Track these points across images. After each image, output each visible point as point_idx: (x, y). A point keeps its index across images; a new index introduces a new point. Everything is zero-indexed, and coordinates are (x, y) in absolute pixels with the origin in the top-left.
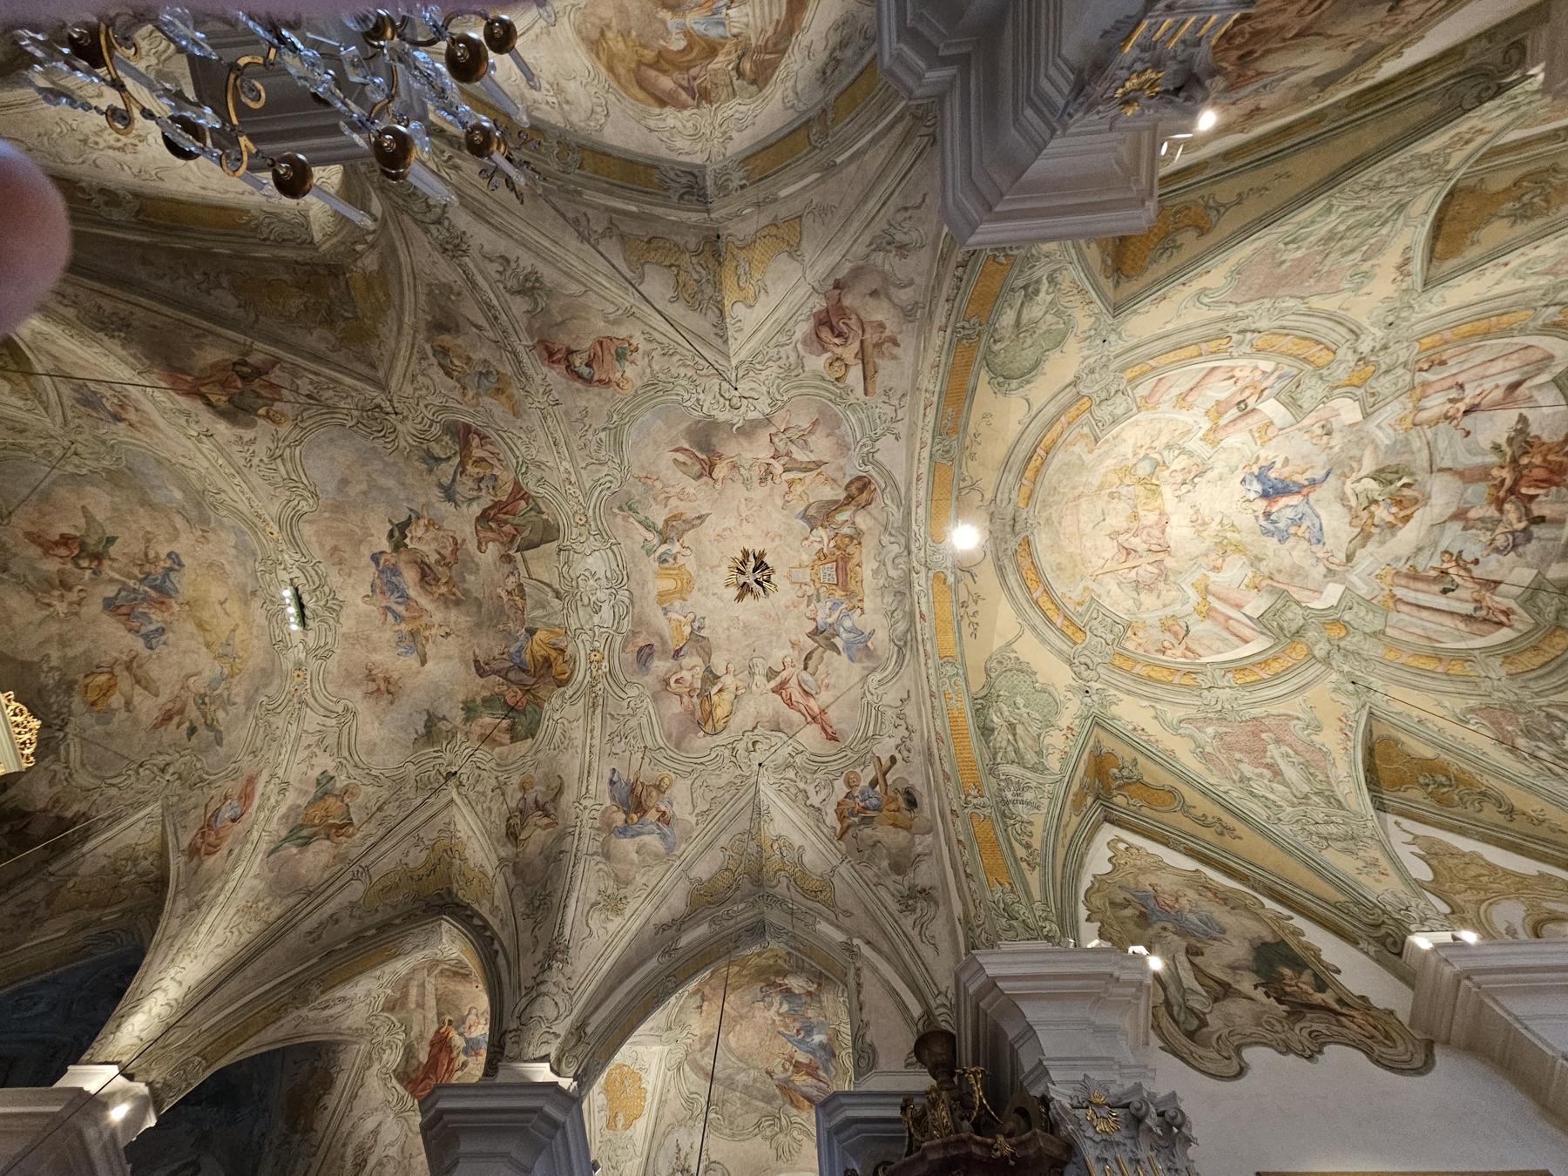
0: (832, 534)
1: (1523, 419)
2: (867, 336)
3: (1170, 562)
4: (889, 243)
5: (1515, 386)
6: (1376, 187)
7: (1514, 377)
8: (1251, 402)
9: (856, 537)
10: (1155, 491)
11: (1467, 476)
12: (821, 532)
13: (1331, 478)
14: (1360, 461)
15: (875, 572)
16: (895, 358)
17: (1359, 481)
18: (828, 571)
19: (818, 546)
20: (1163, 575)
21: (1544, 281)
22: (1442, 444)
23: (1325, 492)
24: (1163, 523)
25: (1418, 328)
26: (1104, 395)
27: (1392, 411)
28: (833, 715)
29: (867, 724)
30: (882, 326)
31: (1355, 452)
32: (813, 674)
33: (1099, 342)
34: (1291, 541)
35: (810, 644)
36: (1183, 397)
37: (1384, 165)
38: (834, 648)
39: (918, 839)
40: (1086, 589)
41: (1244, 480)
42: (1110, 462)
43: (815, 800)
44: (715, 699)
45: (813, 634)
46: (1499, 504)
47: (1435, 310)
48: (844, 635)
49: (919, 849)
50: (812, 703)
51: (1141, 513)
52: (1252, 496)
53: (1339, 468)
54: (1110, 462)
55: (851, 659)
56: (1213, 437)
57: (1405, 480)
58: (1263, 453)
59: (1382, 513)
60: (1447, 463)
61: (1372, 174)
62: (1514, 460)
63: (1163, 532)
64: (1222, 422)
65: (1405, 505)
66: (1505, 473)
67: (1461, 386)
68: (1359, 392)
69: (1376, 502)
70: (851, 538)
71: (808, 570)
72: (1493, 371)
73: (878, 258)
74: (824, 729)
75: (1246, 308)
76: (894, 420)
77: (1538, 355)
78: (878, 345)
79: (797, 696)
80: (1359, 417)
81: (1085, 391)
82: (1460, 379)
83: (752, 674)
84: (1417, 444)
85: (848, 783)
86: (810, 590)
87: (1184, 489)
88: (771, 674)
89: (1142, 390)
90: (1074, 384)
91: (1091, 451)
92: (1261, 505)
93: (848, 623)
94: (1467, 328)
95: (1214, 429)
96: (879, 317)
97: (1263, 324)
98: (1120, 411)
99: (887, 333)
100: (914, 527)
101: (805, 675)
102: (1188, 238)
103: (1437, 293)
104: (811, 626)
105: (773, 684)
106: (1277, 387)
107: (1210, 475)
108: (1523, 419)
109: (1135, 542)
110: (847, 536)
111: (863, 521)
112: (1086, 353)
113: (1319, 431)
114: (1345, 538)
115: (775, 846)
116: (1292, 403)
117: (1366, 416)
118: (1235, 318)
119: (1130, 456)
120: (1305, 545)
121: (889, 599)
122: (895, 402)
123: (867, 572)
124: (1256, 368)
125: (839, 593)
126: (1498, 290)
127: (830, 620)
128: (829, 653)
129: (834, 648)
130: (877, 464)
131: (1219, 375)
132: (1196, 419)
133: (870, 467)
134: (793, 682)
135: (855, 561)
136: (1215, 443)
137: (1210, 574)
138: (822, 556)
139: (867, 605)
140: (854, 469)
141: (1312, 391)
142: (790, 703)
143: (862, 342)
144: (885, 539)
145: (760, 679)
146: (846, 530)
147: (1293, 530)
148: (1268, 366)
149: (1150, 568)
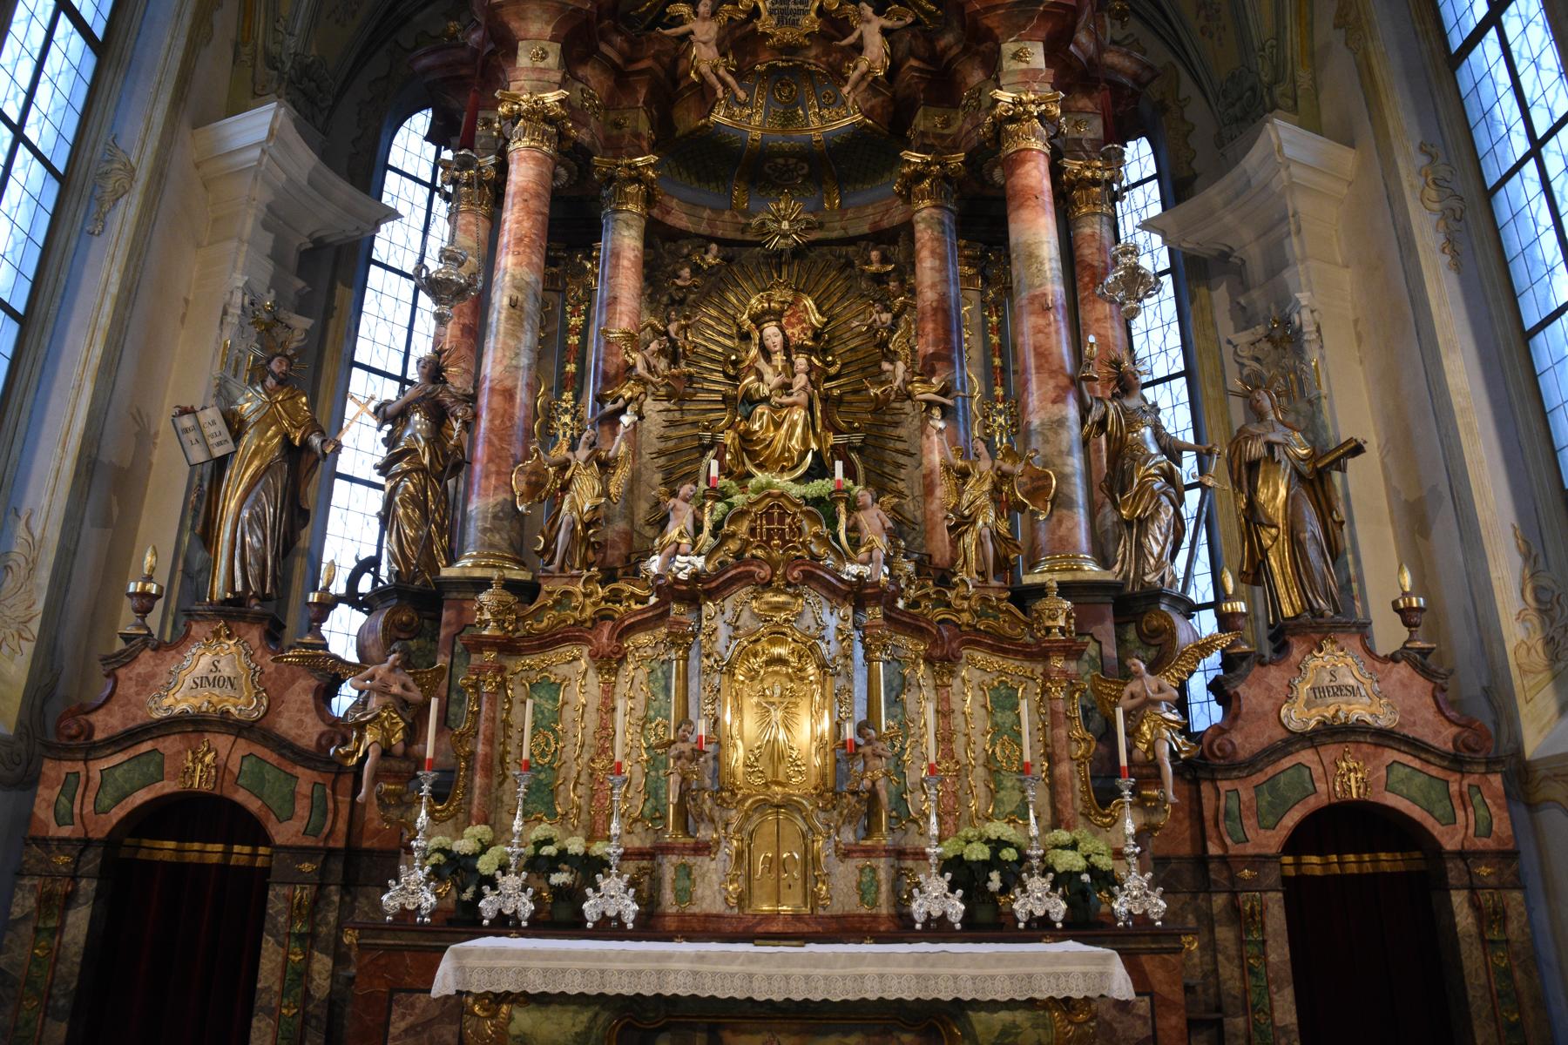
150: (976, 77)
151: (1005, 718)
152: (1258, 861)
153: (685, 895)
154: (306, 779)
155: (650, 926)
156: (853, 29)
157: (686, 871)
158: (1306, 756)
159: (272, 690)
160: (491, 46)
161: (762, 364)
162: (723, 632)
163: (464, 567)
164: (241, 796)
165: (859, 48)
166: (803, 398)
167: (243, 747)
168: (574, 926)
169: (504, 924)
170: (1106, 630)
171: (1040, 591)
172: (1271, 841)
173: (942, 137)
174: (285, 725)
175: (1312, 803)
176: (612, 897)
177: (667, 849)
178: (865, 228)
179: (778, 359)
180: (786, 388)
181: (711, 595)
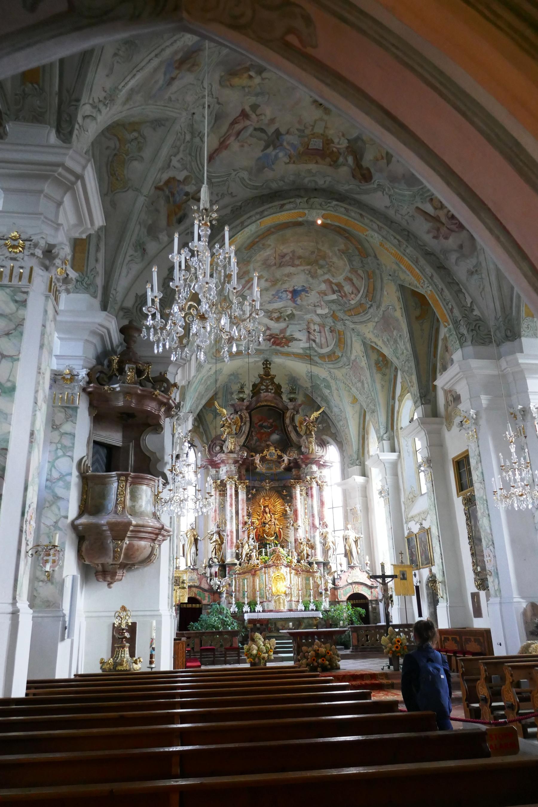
0: (341, 151)
1: (300, 340)
2: (445, 229)
3: (274, 268)
4: (476, 271)
5: (314, 341)
6: (407, 360)
7: (317, 340)
8: (339, 294)
9: (335, 164)
10: (309, 264)
11: (283, 331)
12: (344, 144)
13: (295, 305)
14: (300, 311)
15: (309, 171)
16: (428, 232)
17: (291, 310)
18: (317, 144)
19: (336, 140)
20: (269, 266)
21: (353, 358)
22: (298, 326)
23: (290, 303)
24: (293, 266)
25: (348, 334)
26: (364, 262)
27: (317, 319)
28: (224, 154)
29: (218, 177)
30: (446, 238)
31: (304, 310)
32: (251, 135)
33: (391, 274)
34: (271, 297)
35: (271, 130)
36: (351, 280)
37: (414, 366)
38: (266, 147)
39: (165, 233)
40: (270, 245)
41: (304, 286)
42: (331, 254)
43: (175, 162)
44: (246, 75)
45: (278, 133)
46: (270, 335)
47: (354, 339)
48: (274, 153)
49: (161, 236)
50: (232, 138)
51: (300, 260)
52: (296, 288)
53: (300, 308)
54: (331, 254)
55: (259, 159)
56: (329, 282)
57: (287, 319)
58: (313, 293)
59: (276, 315)
60: (290, 326)
61: (412, 364)
62: (285, 338)
63: (289, 266)
64: (333, 285)
65: (278, 320)
66: (282, 335)
67: (320, 332)
68: (329, 315)
69: (281, 313)
70: (335, 162)
71: (321, 131)
72: (322, 338)
73: (474, 261)
74: (216, 150)
75: (381, 312)
76: (397, 211)
77: (323, 347)
78: (438, 230)
79: (238, 127)
80: (317, 313)
81: (370, 258)
82: (323, 334)
83: (257, 95)
84: (301, 322)
85: (186, 178)
86: (307, 132)
87: (307, 272)
88: (254, 107)
89: (360, 272)
90: (375, 256)
91: (339, 250)
92: (291, 289)
93: (281, 155)
94: (343, 340)
95: (331, 283)
96: (451, 240)
97: (371, 310)
98: (354, 263)
99: (441, 238)
100: (335, 203)
101: (251, 129)
102: (418, 313)
103: (360, 342)
104: (283, 130)
105: (248, 109)
106: (342, 302)
107: (310, 279)
108: (300, 340)
109: (287, 258)
110: (338, 158)
111: (344, 171)
112: (388, 268)
113: (317, 304)
114: (268, 308)
115: (135, 134)
116: (333, 301)
117: (318, 315)
118: (378, 307)
119: (331, 260)
120: (269, 299)
121: (292, 178)
122: (407, 217)
123: (312, 167)
124: (353, 299)
125: (301, 149)
126: (354, 351)
127: (285, 144)
128: (263, 143)
129: (266, 147)
130: (375, 190)
131: (355, 291)
132: (340, 279)
133: (375, 186)
134: (248, 123)
135: (320, 160)
136: (325, 282)
137: (265, 279)
138: (328, 142)
139: (291, 167)
140: (378, 178)
141: (334, 307)
142: (234, 122)
143: (443, 224)
144: (329, 179)
145: (253, 100)
146: (341, 160)
147: (277, 297)
148: (353, 302)
149: (273, 262)
150: (304, 466)
151: (308, 582)
152: (342, 601)
153: (268, 608)
154: (207, 594)
155: (264, 611)
156: (282, 458)
157: (268, 604)
158: (351, 586)
159: (200, 580)
160: (219, 461)
161: (265, 515)
162: (271, 572)
163: (228, 560)
164: (198, 597)
165: (284, 460)
166: (273, 524)
167: (197, 589)
168: (254, 612)
169: (247, 612)
170: (322, 568)
171: (312, 563)
172: (344, 598)
173: (297, 475)
174: (202, 586)
175: (352, 593)
176: (259, 608)
177: (265, 602)
178: (282, 485)
179: (269, 515)
180: (271, 520)
181: (269, 567)
